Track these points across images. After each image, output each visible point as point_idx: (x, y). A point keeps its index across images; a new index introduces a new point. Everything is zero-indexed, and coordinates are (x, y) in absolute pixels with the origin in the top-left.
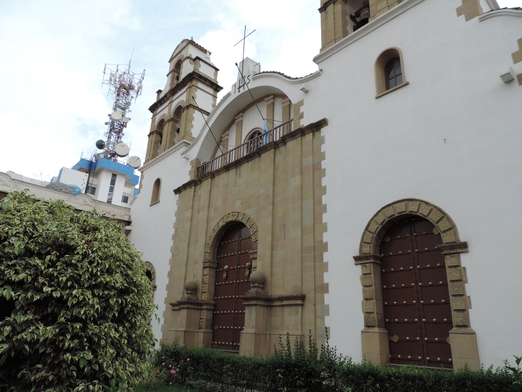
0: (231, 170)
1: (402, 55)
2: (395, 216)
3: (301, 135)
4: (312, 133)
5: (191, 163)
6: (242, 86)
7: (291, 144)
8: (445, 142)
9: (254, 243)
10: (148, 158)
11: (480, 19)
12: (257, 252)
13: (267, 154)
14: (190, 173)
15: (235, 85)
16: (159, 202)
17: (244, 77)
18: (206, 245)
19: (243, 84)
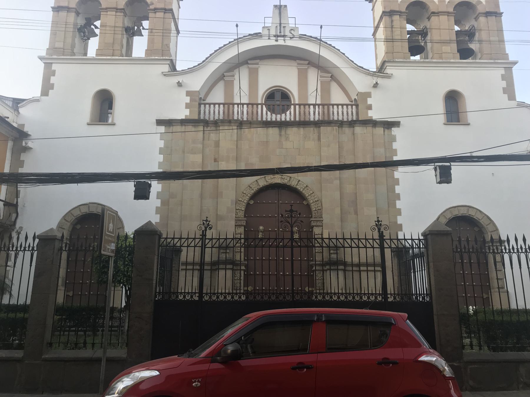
0: (271, 128)
1: (445, 94)
2: (458, 215)
3: (373, 126)
4: (383, 128)
5: (188, 93)
6: (280, 36)
7: (358, 130)
8: (493, 176)
9: (316, 211)
10: (62, 46)
11: (518, 104)
12: (323, 221)
13: (329, 129)
14: (187, 106)
15: (269, 30)
16: (114, 124)
17: (284, 27)
18: (237, 202)
19: (282, 34)
